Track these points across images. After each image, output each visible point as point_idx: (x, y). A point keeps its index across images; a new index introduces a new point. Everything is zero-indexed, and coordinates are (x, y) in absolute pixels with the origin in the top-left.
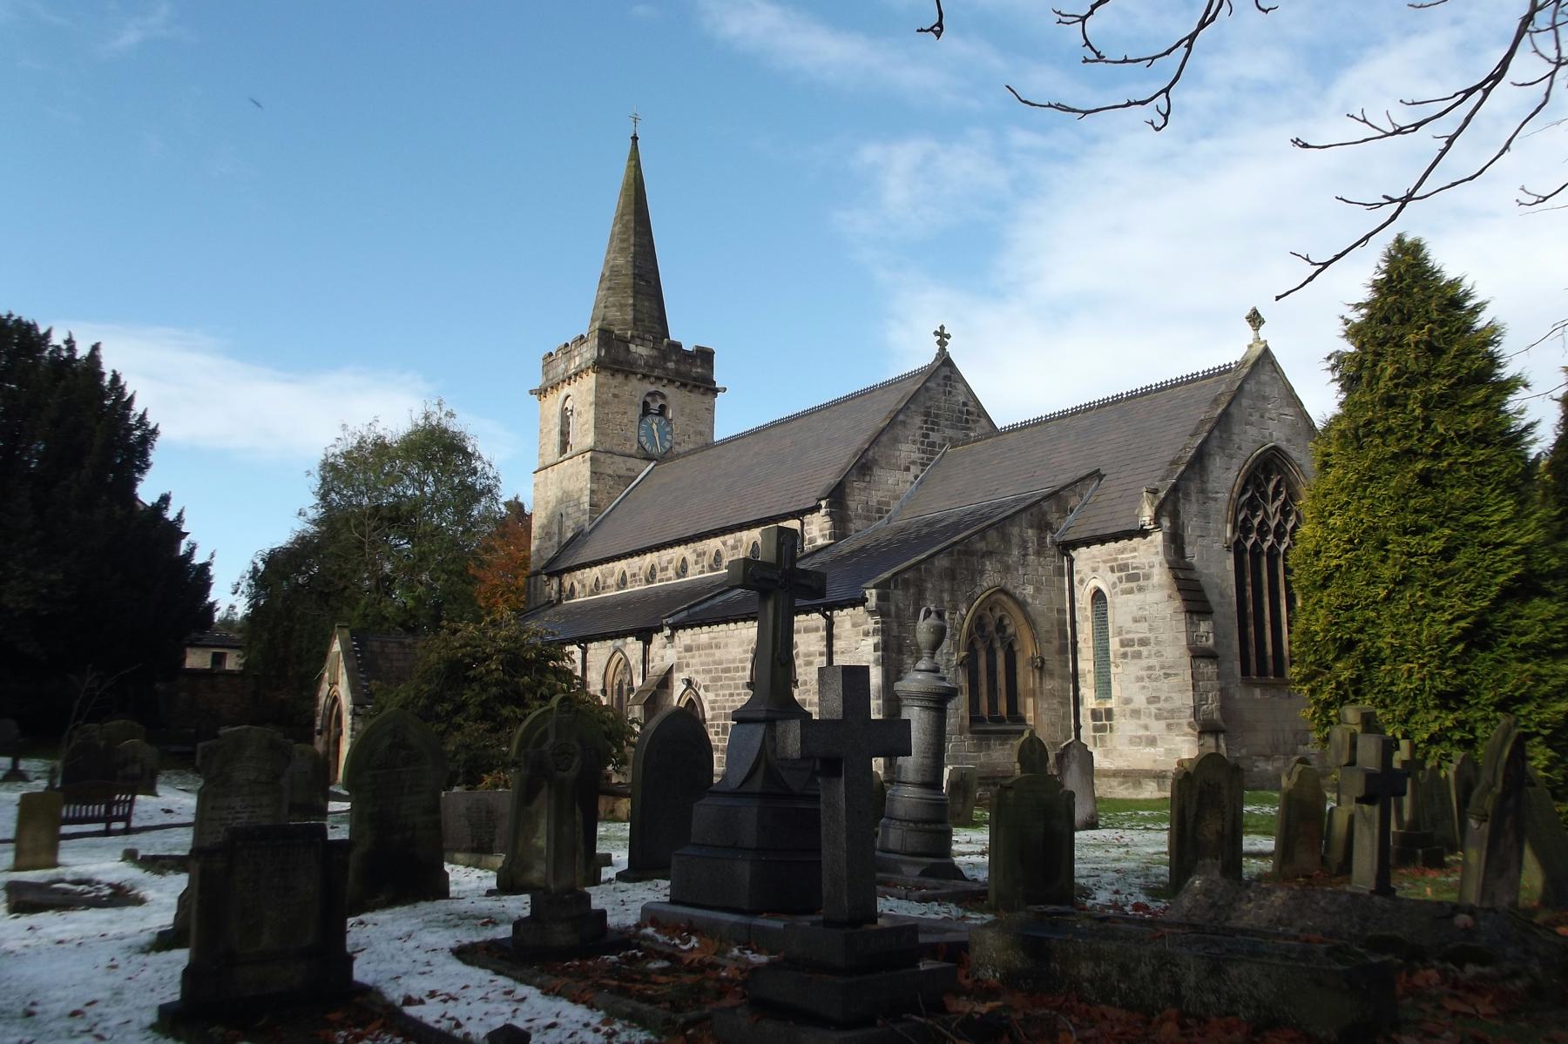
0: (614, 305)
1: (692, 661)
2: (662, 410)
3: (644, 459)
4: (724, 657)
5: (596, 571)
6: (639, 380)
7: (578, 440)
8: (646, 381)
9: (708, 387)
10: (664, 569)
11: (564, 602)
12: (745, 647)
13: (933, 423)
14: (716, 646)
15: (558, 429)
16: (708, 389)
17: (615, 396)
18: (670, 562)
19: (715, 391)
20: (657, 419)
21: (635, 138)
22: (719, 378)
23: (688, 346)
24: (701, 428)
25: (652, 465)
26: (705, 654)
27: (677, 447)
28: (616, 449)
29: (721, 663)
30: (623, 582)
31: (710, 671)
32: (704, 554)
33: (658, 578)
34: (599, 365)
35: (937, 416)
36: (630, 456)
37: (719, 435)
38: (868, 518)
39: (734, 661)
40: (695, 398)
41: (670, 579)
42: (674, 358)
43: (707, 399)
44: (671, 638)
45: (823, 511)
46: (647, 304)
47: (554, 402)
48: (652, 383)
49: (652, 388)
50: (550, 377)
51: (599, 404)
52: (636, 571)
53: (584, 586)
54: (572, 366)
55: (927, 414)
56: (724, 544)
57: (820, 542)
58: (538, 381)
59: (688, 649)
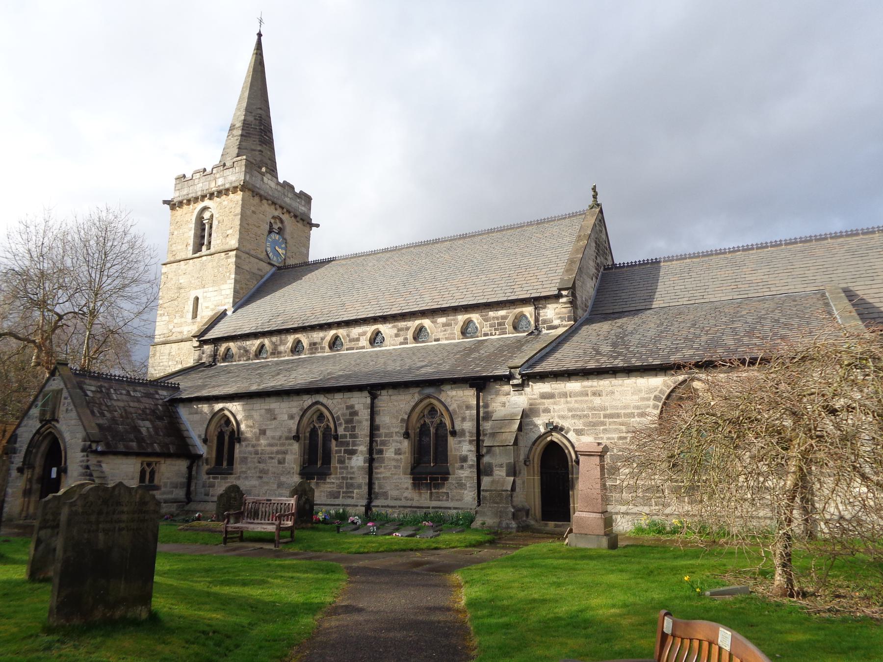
0: (246, 149)
1: (551, 407)
2: (281, 231)
3: (270, 264)
4: (607, 404)
5: (266, 341)
6: (269, 205)
7: (219, 242)
8: (273, 207)
9: (309, 224)
10: (358, 340)
11: (219, 364)
12: (643, 395)
13: (598, 250)
14: (594, 394)
15: (192, 232)
16: (308, 223)
17: (254, 212)
18: (364, 334)
19: (310, 225)
20: (277, 237)
21: (260, 35)
22: (315, 218)
23: (297, 191)
24: (303, 250)
25: (274, 269)
26: (576, 401)
27: (288, 259)
28: (252, 252)
29: (605, 409)
30: (297, 348)
31: (586, 416)
32: (408, 329)
33: (345, 347)
34: (245, 187)
35: (599, 246)
36: (261, 260)
37: (313, 257)
38: (582, 309)
39: (625, 407)
40: (300, 225)
41: (363, 348)
42: (290, 195)
43: (306, 229)
44: (520, 387)
45: (564, 300)
46: (269, 153)
47: (189, 214)
48: (276, 209)
49: (277, 213)
50: (185, 192)
51: (243, 216)
52: (318, 340)
53: (246, 351)
54: (213, 185)
55: (596, 243)
56: (432, 322)
57: (556, 322)
58: (171, 194)
59: (544, 396)
